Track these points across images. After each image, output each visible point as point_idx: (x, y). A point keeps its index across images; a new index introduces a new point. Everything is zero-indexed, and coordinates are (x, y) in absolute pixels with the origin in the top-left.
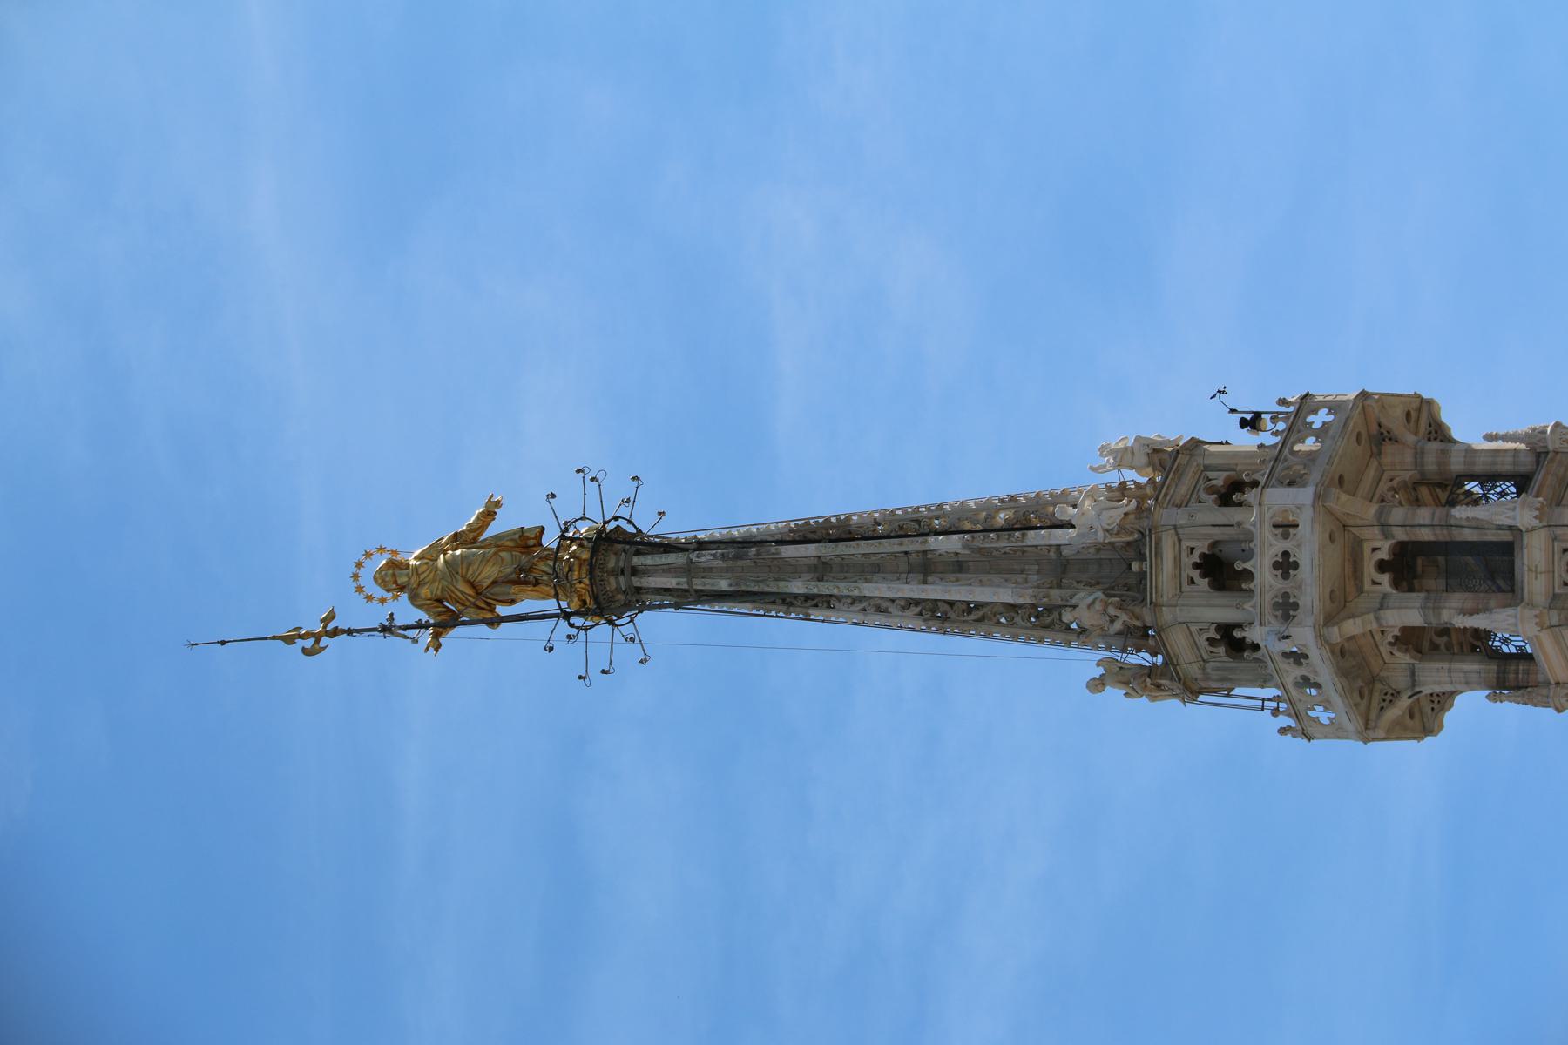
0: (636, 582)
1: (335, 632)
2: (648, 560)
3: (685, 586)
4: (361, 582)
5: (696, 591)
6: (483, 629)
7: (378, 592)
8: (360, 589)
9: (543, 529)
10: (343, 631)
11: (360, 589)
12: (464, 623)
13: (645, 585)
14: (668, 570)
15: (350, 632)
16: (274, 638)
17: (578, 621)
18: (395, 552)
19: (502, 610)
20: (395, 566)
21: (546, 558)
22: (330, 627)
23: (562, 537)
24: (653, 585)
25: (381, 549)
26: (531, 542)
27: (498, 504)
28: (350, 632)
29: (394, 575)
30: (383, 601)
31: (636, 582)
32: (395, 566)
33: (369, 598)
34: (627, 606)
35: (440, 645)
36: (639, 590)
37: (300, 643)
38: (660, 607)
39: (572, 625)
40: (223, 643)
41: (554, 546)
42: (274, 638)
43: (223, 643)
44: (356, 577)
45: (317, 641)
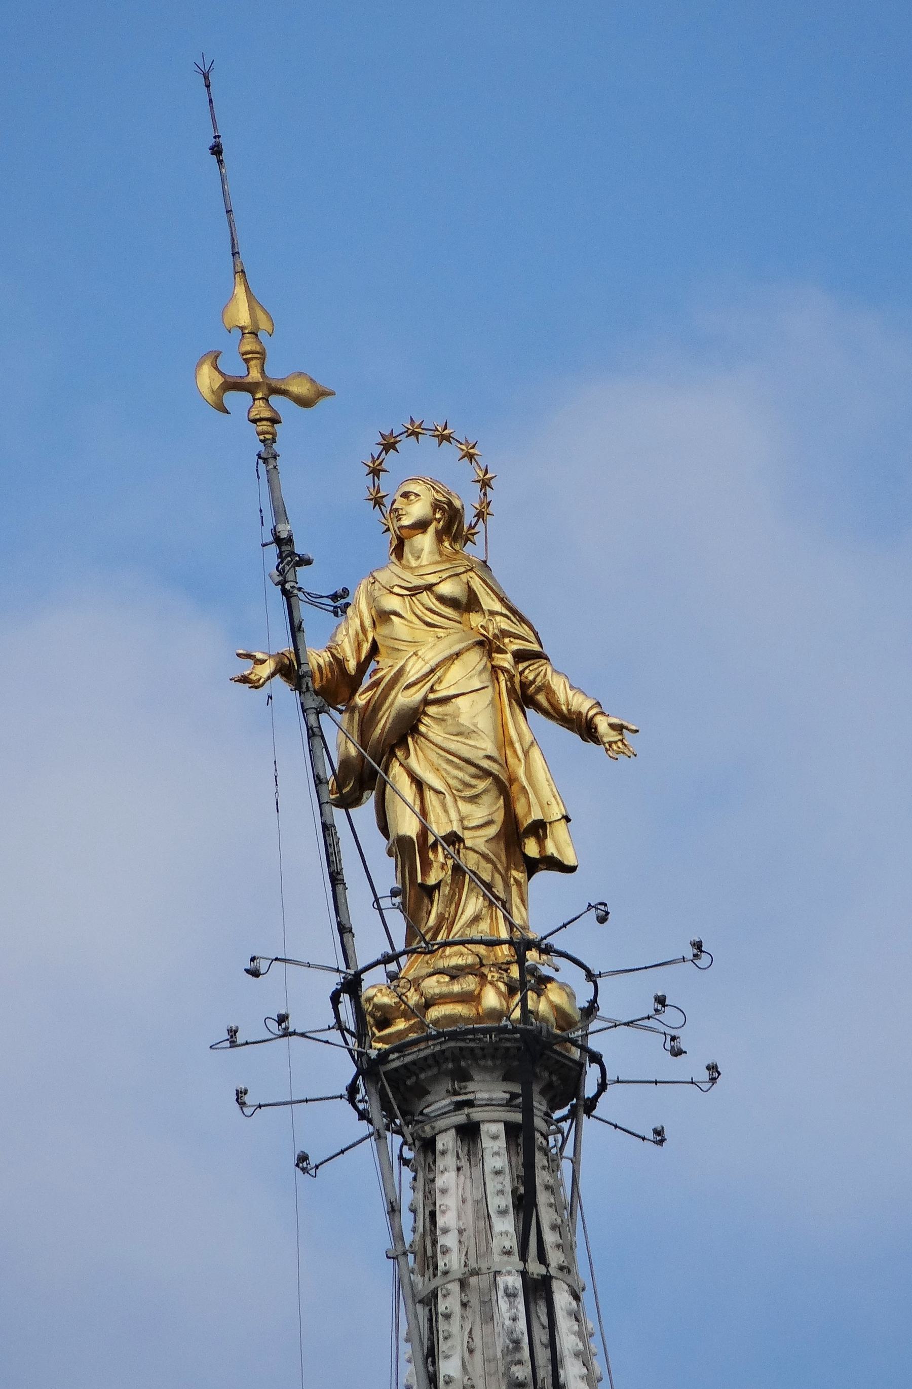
0: (446, 1141)
5: (434, 1295)
24: (439, 1183)
31: (446, 1141)
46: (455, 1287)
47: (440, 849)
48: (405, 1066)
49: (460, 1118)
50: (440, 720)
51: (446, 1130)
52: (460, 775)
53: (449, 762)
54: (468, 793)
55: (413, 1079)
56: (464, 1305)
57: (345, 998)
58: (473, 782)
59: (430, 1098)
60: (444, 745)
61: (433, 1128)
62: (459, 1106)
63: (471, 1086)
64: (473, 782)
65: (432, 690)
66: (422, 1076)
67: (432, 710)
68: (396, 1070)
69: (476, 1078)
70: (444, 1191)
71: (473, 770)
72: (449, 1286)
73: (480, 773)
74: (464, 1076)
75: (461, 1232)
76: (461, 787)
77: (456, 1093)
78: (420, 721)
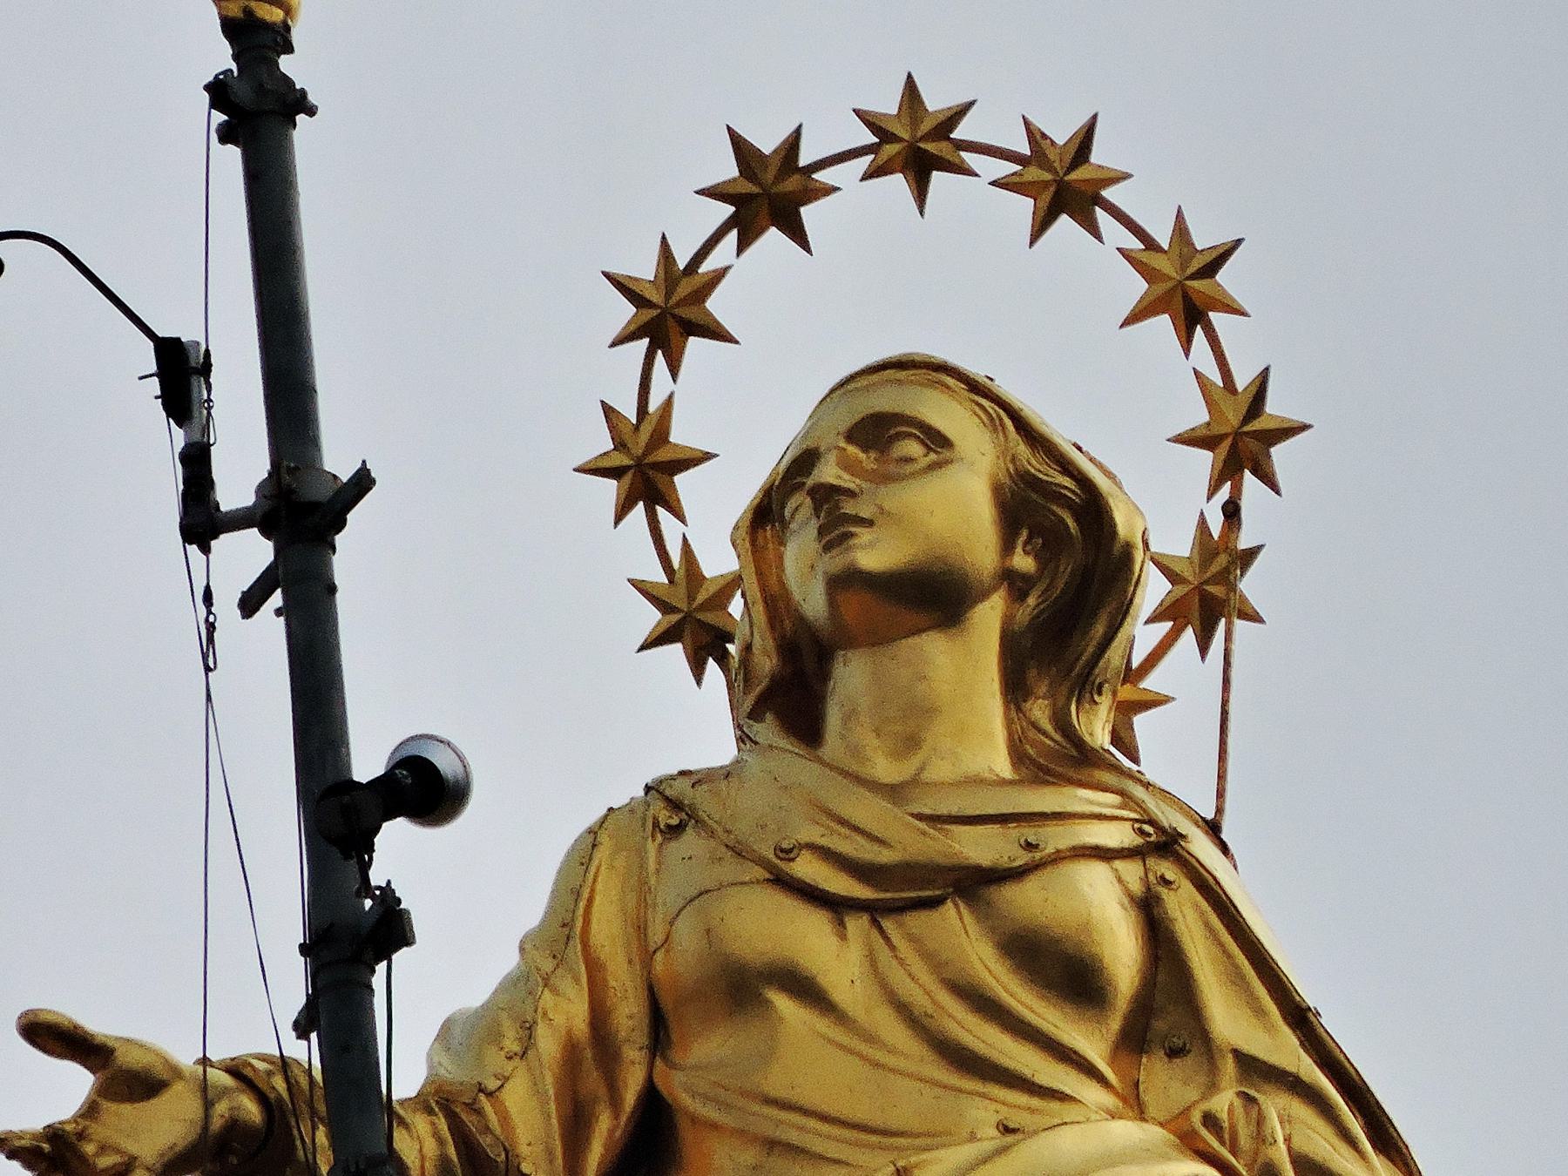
7: (743, 415)
11: (769, 193)
25: (1242, 441)
29: (934, 596)
33: (670, 315)
44: (917, 147)
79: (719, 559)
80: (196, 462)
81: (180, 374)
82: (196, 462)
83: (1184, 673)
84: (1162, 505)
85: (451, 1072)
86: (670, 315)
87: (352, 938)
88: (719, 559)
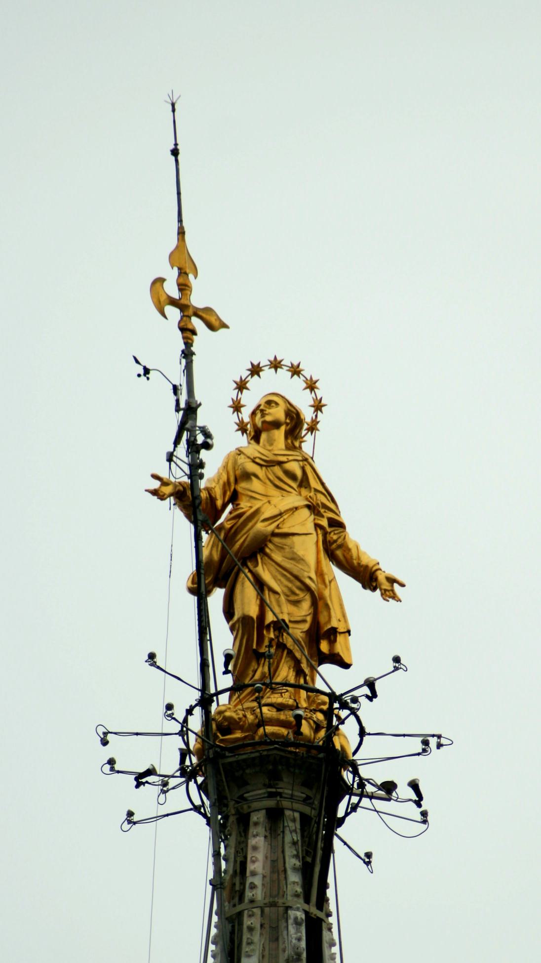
0: (258, 817)
1: (187, 332)
2: (292, 833)
3: (249, 894)
4: (267, 373)
5: (240, 914)
6: (187, 566)
7: (251, 400)
8: (255, 370)
9: (346, 666)
10: (188, 344)
11: (255, 370)
12: (198, 538)
13: (252, 830)
14: (277, 869)
15: (188, 354)
16: (181, 232)
17: (196, 722)
18: (312, 428)
19: (216, 599)
20: (294, 425)
21: (299, 672)
22: (196, 323)
23: (333, 697)
24: (252, 842)
25: (318, 406)
26: (324, 646)
27: (389, 595)
28: (188, 354)
29: (276, 425)
30: (237, 407)
31: (258, 817)
32: (294, 425)
33: (241, 386)
34: (219, 804)
35: (162, 498)
36: (244, 822)
37: (171, 276)
38: (216, 854)
39: (189, 712)
40: (175, 152)
41: (319, 685)
42: (181, 232)
43: (175, 152)
44: (276, 365)
45: (173, 302)
46: (257, 911)
47: (272, 630)
48: (237, 762)
49: (271, 803)
50: (280, 548)
51: (258, 810)
52: (290, 585)
53: (284, 576)
54: (293, 598)
55: (241, 772)
56: (262, 926)
57: (198, 711)
58: (298, 592)
59: (249, 788)
60: (283, 564)
61: (249, 807)
62: (271, 795)
63: (281, 784)
64: (298, 592)
65: (278, 527)
66: (248, 771)
67: (276, 540)
68: (230, 763)
69: (285, 780)
70: (255, 848)
71: (298, 584)
72: (254, 910)
73: (303, 587)
74: (274, 777)
75: (264, 877)
76: (288, 593)
77: (270, 786)
78: (266, 545)
79: (247, 419)
80: (178, 401)
81: (175, 389)
82: (178, 401)
83: (309, 438)
84: (308, 414)
85: (209, 485)
86: (241, 386)
87: (196, 467)
88: (247, 419)
